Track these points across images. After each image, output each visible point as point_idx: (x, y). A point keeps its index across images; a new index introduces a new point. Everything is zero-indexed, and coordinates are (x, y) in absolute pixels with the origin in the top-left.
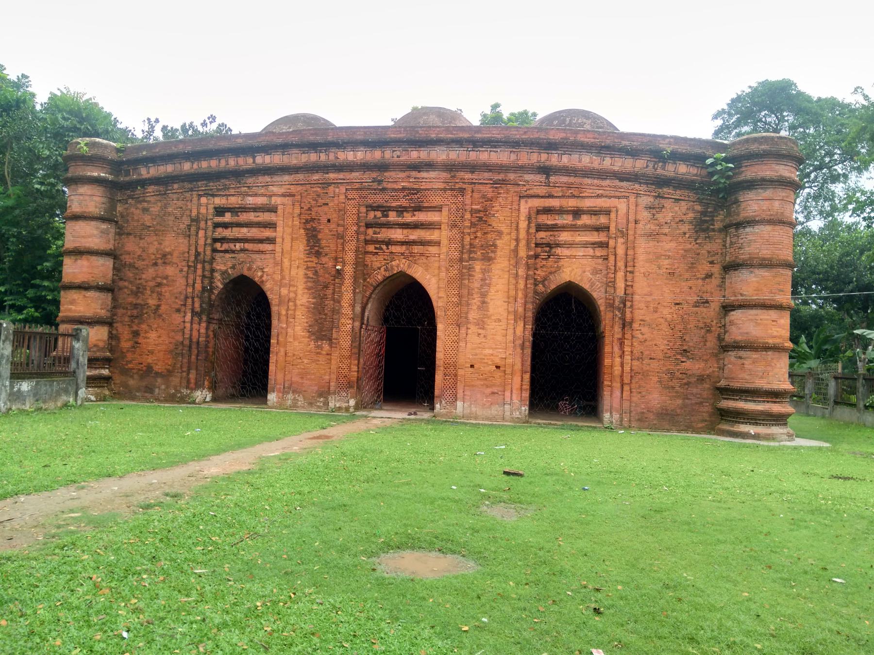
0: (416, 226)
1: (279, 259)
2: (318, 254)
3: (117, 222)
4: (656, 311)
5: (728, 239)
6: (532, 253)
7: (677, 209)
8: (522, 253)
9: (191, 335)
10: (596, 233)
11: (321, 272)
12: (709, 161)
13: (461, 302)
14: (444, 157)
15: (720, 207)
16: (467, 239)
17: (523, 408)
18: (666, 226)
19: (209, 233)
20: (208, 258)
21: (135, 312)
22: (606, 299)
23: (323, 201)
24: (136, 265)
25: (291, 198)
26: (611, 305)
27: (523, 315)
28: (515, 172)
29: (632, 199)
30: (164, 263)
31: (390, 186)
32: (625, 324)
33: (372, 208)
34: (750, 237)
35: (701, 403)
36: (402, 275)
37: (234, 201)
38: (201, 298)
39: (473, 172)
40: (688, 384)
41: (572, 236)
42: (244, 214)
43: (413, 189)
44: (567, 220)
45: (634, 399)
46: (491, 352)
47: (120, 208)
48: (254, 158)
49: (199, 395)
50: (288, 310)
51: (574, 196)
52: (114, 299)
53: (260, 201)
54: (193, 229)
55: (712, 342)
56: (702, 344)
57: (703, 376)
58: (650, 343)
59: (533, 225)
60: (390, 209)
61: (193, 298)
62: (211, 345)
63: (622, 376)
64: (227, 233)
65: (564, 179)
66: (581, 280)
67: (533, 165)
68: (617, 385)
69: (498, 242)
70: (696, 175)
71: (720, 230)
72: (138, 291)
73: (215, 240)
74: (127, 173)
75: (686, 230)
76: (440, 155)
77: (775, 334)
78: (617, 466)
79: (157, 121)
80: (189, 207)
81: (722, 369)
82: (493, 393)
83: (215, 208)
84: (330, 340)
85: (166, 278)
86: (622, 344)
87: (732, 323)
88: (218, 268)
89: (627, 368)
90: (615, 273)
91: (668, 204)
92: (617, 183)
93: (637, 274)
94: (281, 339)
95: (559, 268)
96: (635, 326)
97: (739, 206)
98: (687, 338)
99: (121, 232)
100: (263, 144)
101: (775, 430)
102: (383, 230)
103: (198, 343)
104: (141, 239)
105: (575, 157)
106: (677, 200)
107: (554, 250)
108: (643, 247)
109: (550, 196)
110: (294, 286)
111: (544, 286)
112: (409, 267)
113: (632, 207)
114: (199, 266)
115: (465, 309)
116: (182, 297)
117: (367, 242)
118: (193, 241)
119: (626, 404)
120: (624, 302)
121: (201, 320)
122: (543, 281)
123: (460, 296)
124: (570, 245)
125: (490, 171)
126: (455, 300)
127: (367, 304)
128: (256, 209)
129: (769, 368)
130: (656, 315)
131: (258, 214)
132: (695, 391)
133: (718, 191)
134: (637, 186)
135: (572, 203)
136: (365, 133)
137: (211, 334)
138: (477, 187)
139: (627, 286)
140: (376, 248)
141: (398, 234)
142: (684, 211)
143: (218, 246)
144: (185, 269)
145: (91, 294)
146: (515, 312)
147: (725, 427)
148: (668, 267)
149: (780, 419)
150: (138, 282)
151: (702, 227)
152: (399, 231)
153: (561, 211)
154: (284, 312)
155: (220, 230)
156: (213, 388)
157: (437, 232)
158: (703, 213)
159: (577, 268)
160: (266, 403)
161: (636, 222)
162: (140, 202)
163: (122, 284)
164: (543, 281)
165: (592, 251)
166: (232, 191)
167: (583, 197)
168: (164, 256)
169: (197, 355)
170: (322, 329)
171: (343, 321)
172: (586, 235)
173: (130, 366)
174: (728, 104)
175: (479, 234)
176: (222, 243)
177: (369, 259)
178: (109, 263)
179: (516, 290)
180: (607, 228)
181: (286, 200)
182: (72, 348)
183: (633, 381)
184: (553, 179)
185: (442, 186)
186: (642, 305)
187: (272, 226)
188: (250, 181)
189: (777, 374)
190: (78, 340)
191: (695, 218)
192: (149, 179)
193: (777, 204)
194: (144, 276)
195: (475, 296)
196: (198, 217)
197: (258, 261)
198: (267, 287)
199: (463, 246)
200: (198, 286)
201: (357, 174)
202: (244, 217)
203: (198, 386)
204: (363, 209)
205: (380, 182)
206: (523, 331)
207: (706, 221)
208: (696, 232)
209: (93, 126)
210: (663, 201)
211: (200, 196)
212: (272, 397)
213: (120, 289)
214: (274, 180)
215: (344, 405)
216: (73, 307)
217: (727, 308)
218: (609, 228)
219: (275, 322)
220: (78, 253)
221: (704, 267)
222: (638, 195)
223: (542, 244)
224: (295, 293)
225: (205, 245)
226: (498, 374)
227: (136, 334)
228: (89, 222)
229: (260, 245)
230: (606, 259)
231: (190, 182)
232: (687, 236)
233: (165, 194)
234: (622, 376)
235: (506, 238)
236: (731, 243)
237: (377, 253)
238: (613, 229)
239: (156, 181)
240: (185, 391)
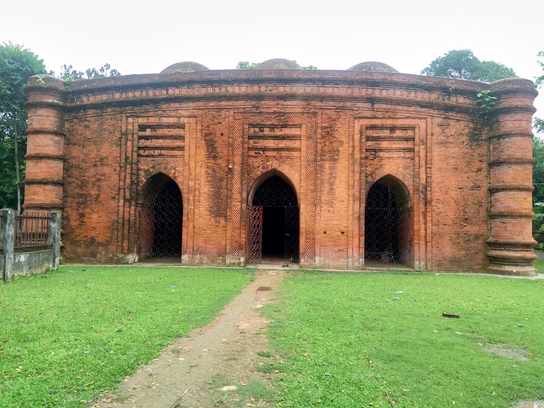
1: (187, 161)
2: (215, 158)
3: (65, 135)
4: (446, 193)
5: (492, 146)
6: (363, 156)
7: (458, 126)
9: (124, 216)
10: (405, 142)
11: (217, 170)
12: (479, 95)
13: (316, 189)
15: (485, 125)
16: (319, 146)
17: (361, 260)
18: (452, 137)
19: (135, 143)
20: (135, 161)
21: (81, 200)
22: (414, 186)
23: (218, 121)
24: (81, 166)
25: (195, 119)
26: (417, 190)
27: (358, 197)
28: (351, 101)
29: (429, 120)
30: (102, 165)
31: (264, 110)
32: (427, 202)
34: (508, 145)
35: (477, 253)
36: (274, 171)
37: (153, 120)
38: (130, 189)
39: (322, 101)
40: (469, 240)
41: (390, 144)
42: (161, 130)
43: (281, 113)
44: (386, 133)
45: (434, 251)
46: (337, 222)
47: (67, 125)
48: (167, 90)
50: (194, 196)
51: (391, 118)
52: (65, 191)
53: (172, 120)
54: (123, 140)
55: (483, 213)
56: (477, 214)
57: (478, 235)
58: (444, 214)
59: (364, 137)
60: (265, 126)
61: (124, 189)
62: (137, 222)
63: (426, 237)
64: (148, 143)
65: (384, 106)
66: (397, 173)
67: (363, 96)
68: (422, 242)
69: (340, 149)
70: (470, 104)
71: (486, 140)
72: (83, 185)
73: (139, 148)
74: (72, 101)
75: (464, 140)
76: (299, 89)
77: (526, 207)
78: (422, 295)
79: (71, 67)
80: (120, 125)
81: (490, 230)
82: (340, 250)
83: (139, 125)
84: (226, 216)
85: (104, 175)
86: (425, 215)
87: (497, 200)
88: (142, 167)
89: (429, 231)
90: (419, 169)
91: (452, 123)
92: (419, 109)
93: (433, 169)
94: (190, 217)
95: (382, 166)
96: (434, 203)
97: (500, 124)
98: (467, 210)
99: (68, 143)
100: (175, 80)
101: (528, 269)
102: (260, 140)
103: (129, 221)
104: (84, 147)
105: (391, 91)
106: (458, 120)
107: (378, 154)
108: (437, 152)
109: (375, 118)
110: (199, 180)
111: (372, 178)
112: (279, 165)
113: (429, 125)
114: (128, 166)
115: (319, 194)
116: (116, 189)
117: (249, 149)
118: (123, 149)
120: (426, 188)
121: (130, 204)
122: (371, 174)
123: (315, 185)
124: (389, 150)
125: (334, 100)
126: (312, 188)
127: (250, 191)
128: (169, 126)
129: (523, 229)
130: (446, 196)
131: (170, 130)
132: (473, 245)
133: (484, 115)
134: (432, 111)
135: (389, 122)
136: (247, 74)
137: (137, 214)
138: (325, 111)
139: (427, 177)
140: (256, 153)
141: (271, 143)
142: (462, 127)
143: (142, 152)
144: (118, 169)
147: (495, 268)
148: (454, 164)
150: (83, 178)
151: (474, 138)
153: (382, 128)
154: (191, 198)
155: (143, 141)
156: (139, 253)
158: (475, 129)
160: (180, 262)
161: (432, 135)
162: (83, 121)
163: (70, 180)
164: (371, 174)
165: (403, 154)
166: (151, 114)
167: (397, 118)
168: (102, 159)
169: (129, 229)
170: (219, 209)
171: (234, 203)
172: (399, 144)
173: (78, 238)
174: (430, 65)
175: (327, 143)
176: (145, 150)
177: (251, 160)
178: (59, 165)
179: (354, 181)
180: (413, 139)
181: (191, 120)
182: (48, 228)
183: (433, 240)
184: (376, 106)
186: (437, 190)
187: (181, 138)
188: (164, 106)
190: (54, 222)
191: (469, 132)
192: (89, 105)
193: (524, 123)
194: (87, 174)
195: (325, 185)
196: (127, 132)
197: (172, 162)
198: (179, 181)
199: (316, 151)
200: (128, 181)
201: (242, 102)
202: (160, 132)
203: (130, 251)
204: (246, 127)
205: (258, 108)
206: (358, 208)
207: (477, 134)
208: (471, 141)
209: (31, 68)
210: (449, 121)
211: (128, 117)
212: (185, 257)
213: (69, 183)
214: (182, 106)
215: (237, 261)
216: (36, 197)
217: (492, 191)
218: (414, 138)
219: (185, 205)
220: (39, 157)
221: (477, 164)
223: (370, 150)
224: (200, 184)
225: (133, 151)
226: (343, 237)
227: (82, 215)
228: (46, 135)
229: (172, 151)
231: (120, 107)
232: (465, 144)
233: (102, 115)
234: (426, 237)
235: (346, 146)
236: (494, 148)
237: (256, 157)
240: (120, 256)
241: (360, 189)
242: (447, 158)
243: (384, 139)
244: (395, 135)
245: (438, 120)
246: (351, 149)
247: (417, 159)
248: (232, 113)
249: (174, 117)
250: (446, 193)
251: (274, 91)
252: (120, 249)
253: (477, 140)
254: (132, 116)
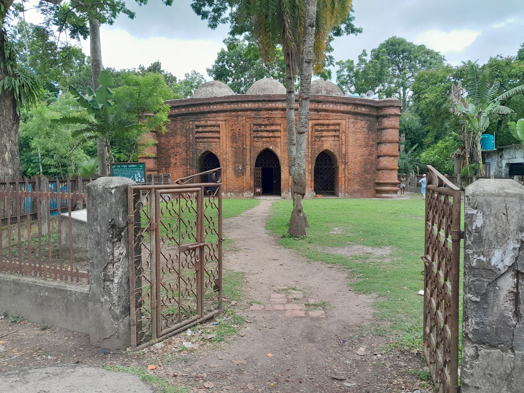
0: (273, 131)
2: (236, 142)
4: (356, 158)
29: (347, 120)
32: (345, 164)
34: (386, 133)
37: (203, 123)
44: (325, 128)
53: (213, 123)
64: (201, 135)
65: (324, 113)
73: (196, 138)
91: (359, 121)
92: (342, 114)
101: (394, 195)
105: (327, 105)
106: (362, 120)
113: (347, 123)
128: (211, 126)
134: (348, 115)
135: (327, 122)
141: (265, 134)
145: (151, 160)
147: (378, 195)
149: (395, 192)
153: (323, 125)
157: (279, 133)
159: (328, 144)
180: (339, 130)
181: (223, 123)
184: (320, 113)
186: (351, 156)
188: (208, 115)
189: (394, 177)
204: (252, 125)
217: (379, 157)
230: (339, 141)
238: (341, 131)
242: (356, 140)
244: (329, 128)
248: (244, 118)
249: (213, 120)
250: (356, 158)
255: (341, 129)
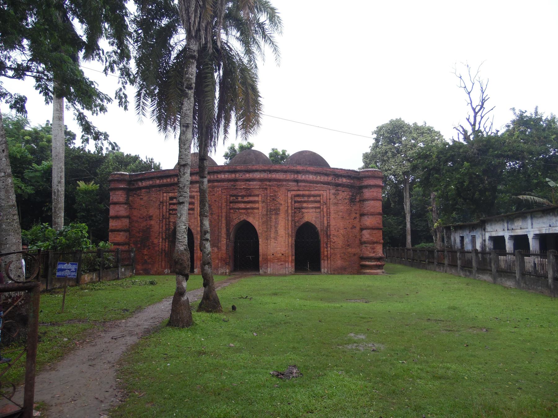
8: (290, 211)
14: (259, 176)
20: (167, 217)
32: (328, 236)
33: (231, 196)
36: (244, 220)
44: (306, 199)
47: (130, 199)
49: (166, 271)
52: (130, 234)
55: (357, 242)
60: (239, 196)
65: (304, 184)
69: (281, 208)
73: (170, 210)
74: (134, 185)
76: (257, 175)
81: (361, 250)
89: (329, 252)
91: (340, 192)
96: (331, 237)
101: (379, 271)
103: (165, 250)
105: (307, 176)
108: (332, 208)
109: (299, 190)
114: (164, 220)
117: (230, 209)
118: (161, 211)
119: (329, 265)
124: (307, 208)
135: (307, 193)
141: (242, 205)
145: (121, 233)
146: (288, 233)
151: (352, 200)
152: (243, 204)
153: (303, 196)
156: (170, 268)
158: (352, 196)
159: (310, 216)
184: (299, 184)
185: (258, 187)
186: (333, 229)
189: (379, 251)
199: (268, 209)
200: (164, 228)
204: (228, 197)
217: (362, 229)
220: (117, 217)
222: (330, 190)
238: (322, 202)
239: (146, 187)
241: (292, 230)
243: (305, 202)
245: (333, 191)
246: (286, 208)
247: (322, 212)
251: (244, 177)
252: (160, 266)
253: (353, 202)
254: (166, 192)
255: (322, 201)
